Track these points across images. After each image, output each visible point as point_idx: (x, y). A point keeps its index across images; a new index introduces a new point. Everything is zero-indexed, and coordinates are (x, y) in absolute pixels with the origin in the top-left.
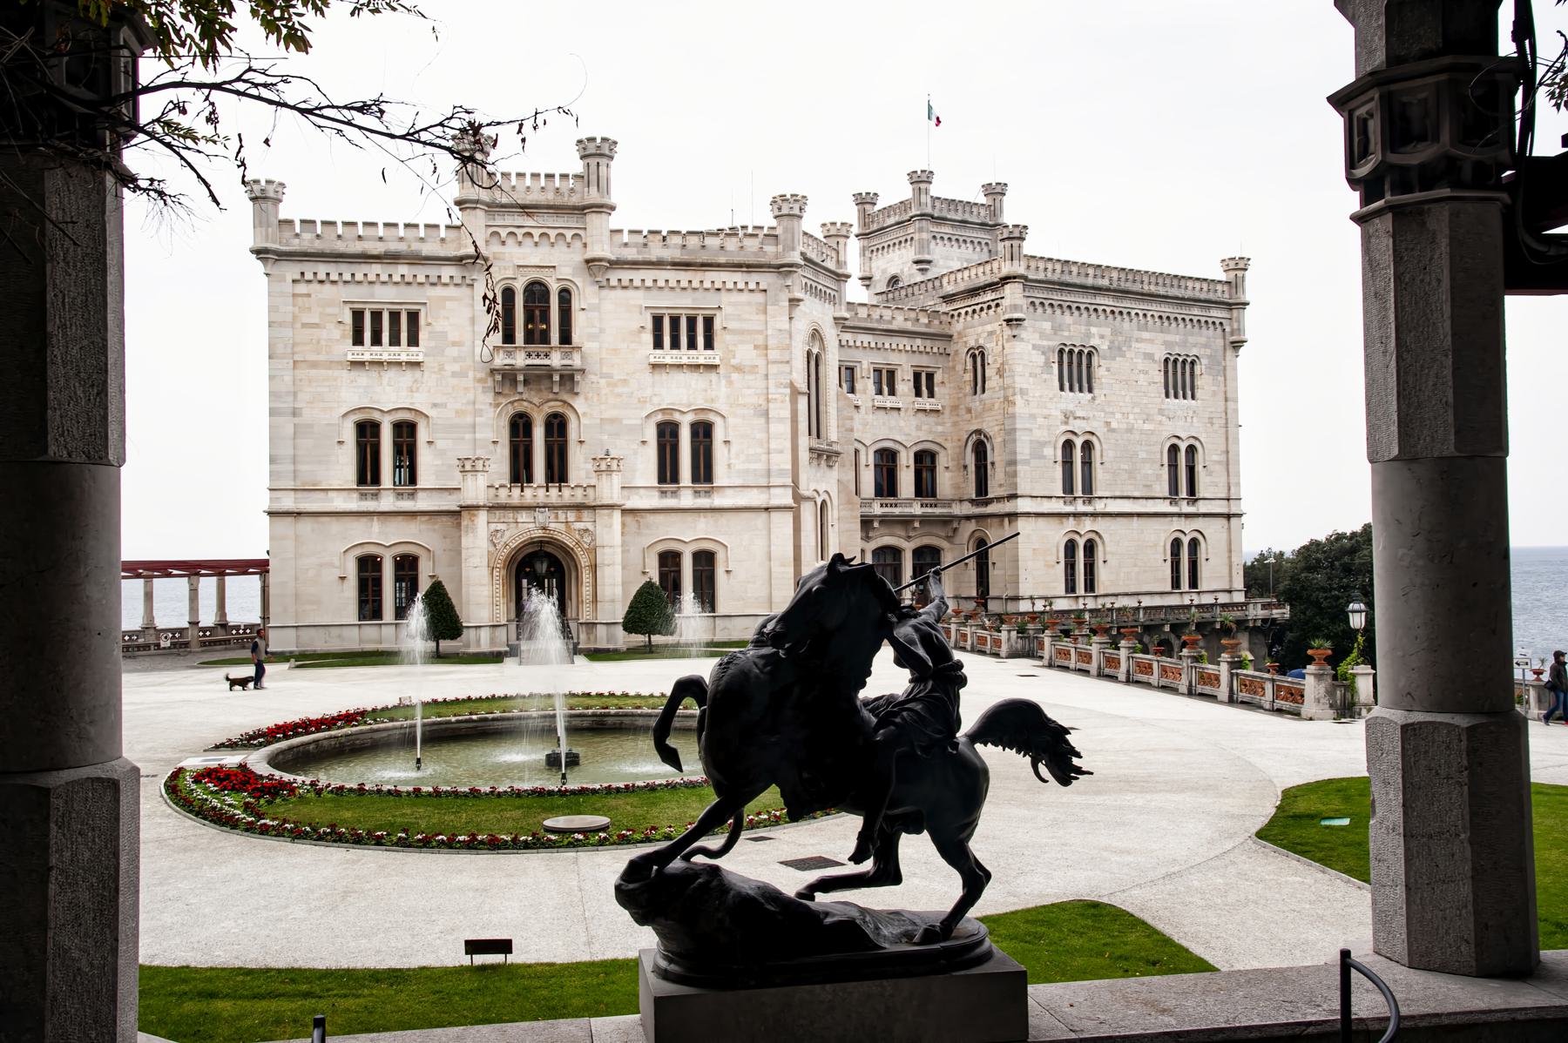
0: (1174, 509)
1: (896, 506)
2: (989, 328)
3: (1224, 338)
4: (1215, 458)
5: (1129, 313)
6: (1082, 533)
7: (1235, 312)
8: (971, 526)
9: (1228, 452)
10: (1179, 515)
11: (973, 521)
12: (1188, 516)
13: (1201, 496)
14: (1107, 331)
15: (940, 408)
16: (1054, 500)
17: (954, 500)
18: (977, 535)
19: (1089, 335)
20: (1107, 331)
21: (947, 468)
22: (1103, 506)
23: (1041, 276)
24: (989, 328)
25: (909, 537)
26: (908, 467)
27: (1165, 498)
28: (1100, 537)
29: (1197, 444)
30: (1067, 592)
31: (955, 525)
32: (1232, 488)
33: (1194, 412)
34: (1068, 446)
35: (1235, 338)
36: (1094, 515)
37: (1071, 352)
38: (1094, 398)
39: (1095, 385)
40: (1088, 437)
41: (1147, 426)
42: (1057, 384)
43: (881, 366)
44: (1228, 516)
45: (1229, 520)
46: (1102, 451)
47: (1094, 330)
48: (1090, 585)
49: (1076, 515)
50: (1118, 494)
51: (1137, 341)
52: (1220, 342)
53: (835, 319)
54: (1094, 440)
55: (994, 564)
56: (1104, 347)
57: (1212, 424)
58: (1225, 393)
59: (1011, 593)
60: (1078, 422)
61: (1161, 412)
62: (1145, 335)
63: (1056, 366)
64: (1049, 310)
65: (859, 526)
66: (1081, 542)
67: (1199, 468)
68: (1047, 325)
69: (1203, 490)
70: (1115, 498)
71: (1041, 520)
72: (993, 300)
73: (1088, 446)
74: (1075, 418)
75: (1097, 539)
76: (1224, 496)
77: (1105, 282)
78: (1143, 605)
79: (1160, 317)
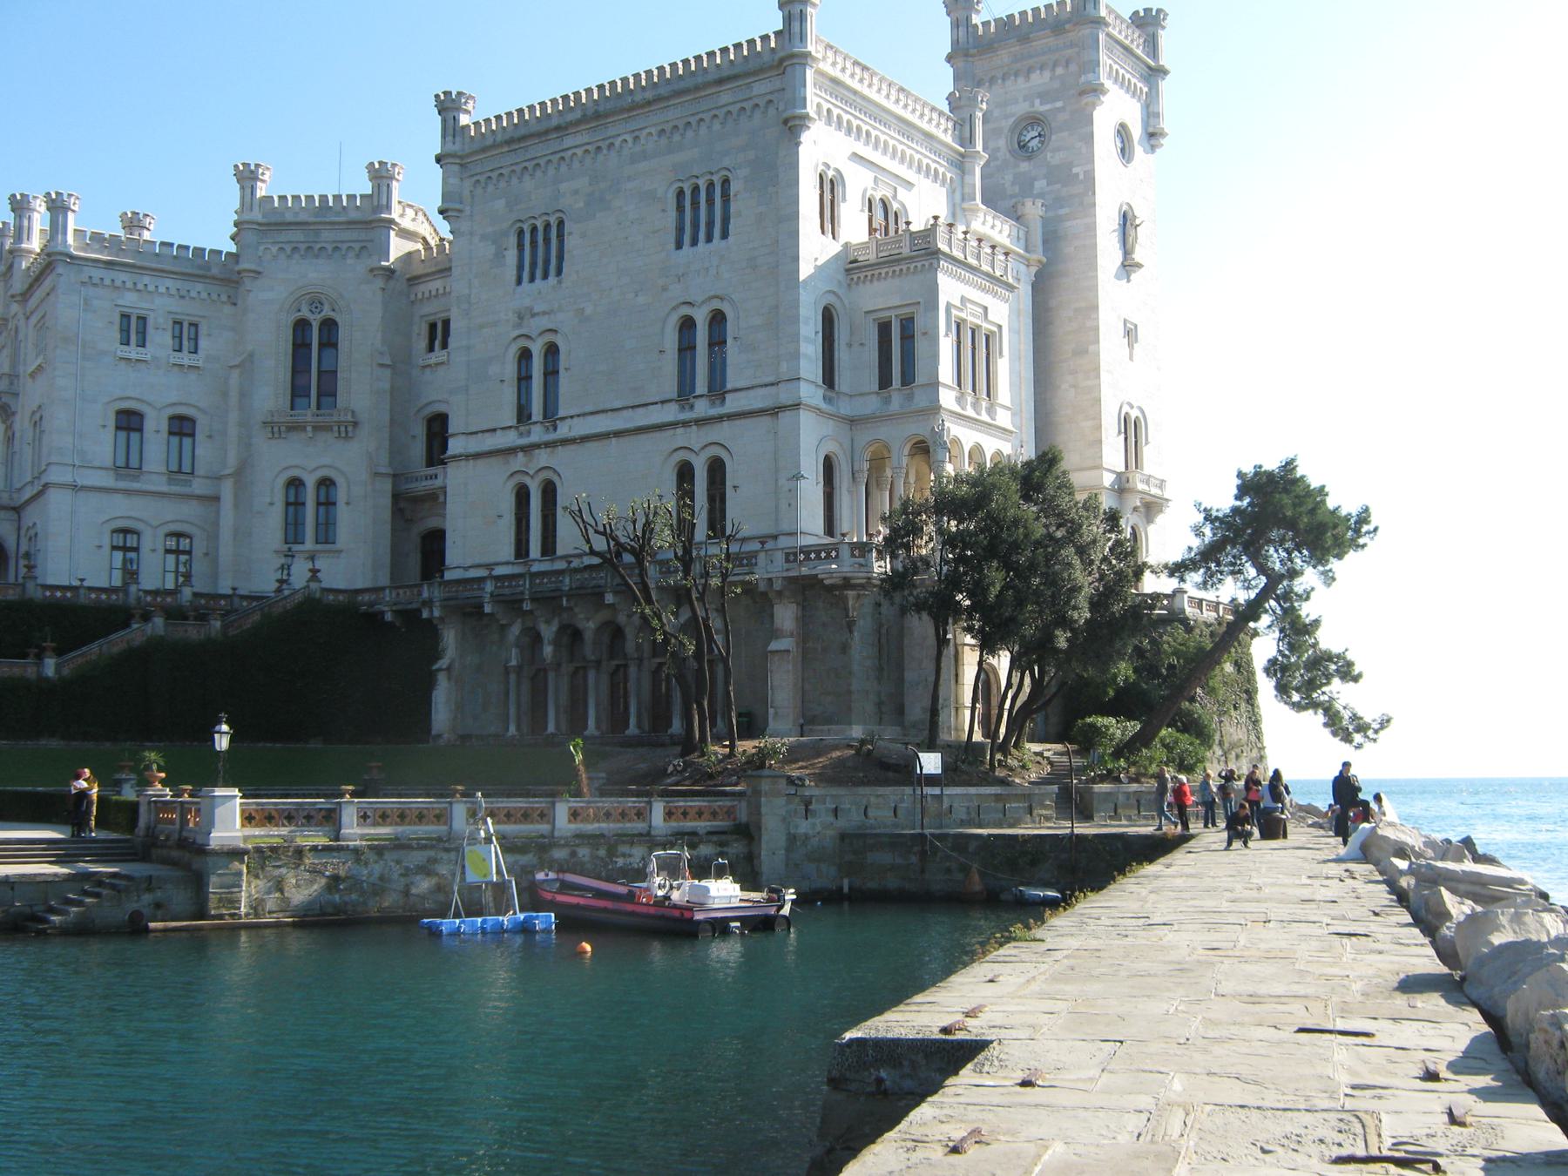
0: (687, 415)
6: (531, 473)
9: (777, 307)
10: (685, 424)
12: (701, 422)
16: (499, 433)
23: (489, 142)
27: (663, 402)
32: (784, 367)
37: (534, 229)
38: (560, 282)
41: (641, 299)
42: (511, 273)
44: (774, 411)
47: (563, 187)
48: (549, 547)
51: (629, 178)
53: (372, 270)
62: (643, 166)
63: (511, 256)
65: (387, 501)
68: (500, 204)
70: (584, 415)
71: (481, 463)
73: (552, 351)
74: (533, 315)
75: (555, 479)
78: (572, 565)
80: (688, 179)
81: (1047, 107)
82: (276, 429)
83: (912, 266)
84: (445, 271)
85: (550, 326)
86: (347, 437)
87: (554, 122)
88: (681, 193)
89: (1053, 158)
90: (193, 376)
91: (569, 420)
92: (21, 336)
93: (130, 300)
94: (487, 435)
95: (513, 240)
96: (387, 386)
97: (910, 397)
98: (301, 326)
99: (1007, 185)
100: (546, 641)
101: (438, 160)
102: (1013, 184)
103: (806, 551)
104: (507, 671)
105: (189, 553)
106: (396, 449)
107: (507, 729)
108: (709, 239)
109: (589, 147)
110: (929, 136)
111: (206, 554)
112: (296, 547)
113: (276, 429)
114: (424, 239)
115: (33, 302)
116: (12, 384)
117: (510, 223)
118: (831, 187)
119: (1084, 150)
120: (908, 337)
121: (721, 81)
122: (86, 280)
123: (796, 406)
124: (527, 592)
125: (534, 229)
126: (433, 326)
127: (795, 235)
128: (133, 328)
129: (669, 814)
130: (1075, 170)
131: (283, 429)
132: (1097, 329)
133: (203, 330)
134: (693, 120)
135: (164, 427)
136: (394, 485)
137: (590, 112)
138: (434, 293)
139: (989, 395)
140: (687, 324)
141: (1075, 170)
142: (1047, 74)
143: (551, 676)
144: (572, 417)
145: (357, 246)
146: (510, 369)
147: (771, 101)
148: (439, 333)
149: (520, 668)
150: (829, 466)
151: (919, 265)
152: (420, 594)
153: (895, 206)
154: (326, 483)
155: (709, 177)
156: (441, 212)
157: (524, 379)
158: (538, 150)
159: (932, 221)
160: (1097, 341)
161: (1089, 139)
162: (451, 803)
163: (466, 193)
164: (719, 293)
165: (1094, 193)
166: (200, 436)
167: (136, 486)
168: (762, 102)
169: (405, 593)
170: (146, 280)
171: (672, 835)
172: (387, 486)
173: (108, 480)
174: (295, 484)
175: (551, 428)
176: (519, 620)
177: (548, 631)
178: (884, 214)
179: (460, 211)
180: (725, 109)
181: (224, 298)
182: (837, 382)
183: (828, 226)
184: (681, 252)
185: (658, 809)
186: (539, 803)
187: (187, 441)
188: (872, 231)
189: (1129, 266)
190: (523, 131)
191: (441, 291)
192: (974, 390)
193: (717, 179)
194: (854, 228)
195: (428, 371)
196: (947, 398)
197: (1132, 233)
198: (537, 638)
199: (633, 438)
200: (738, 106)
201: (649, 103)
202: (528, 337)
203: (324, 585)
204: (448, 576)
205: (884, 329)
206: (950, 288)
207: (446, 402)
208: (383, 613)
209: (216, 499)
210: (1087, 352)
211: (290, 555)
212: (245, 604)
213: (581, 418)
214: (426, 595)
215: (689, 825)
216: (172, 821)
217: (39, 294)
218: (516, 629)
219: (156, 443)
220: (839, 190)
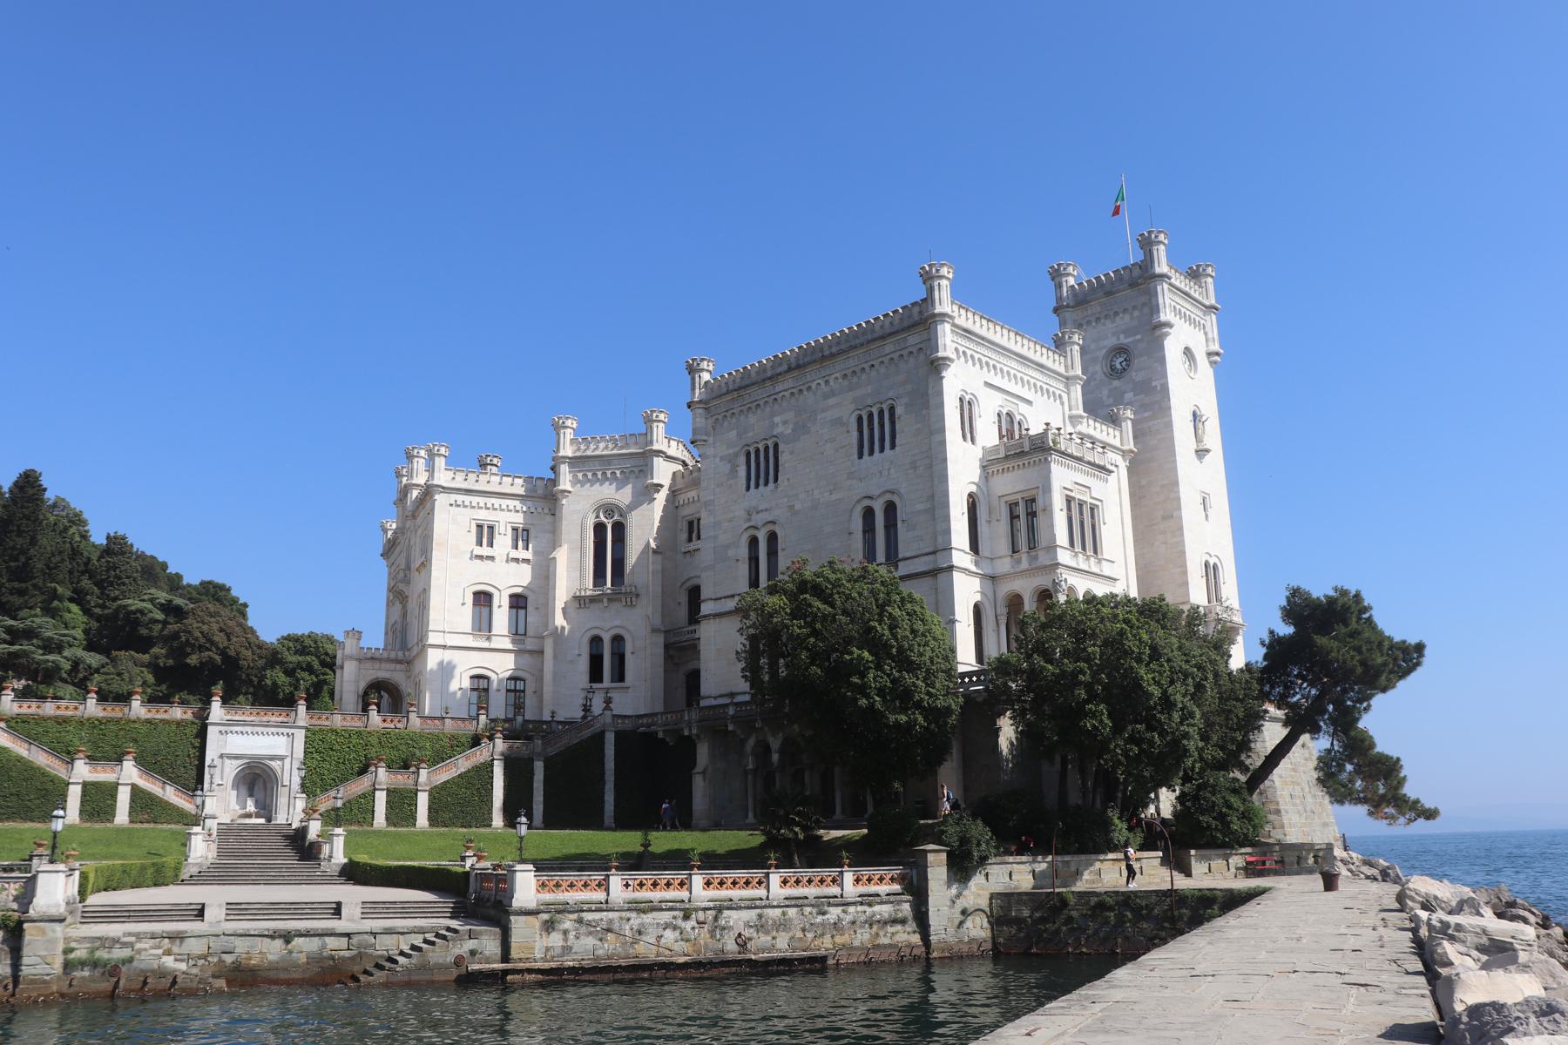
4: (920, 507)
5: (809, 388)
9: (932, 497)
14: (790, 415)
19: (773, 425)
20: (790, 415)
29: (895, 499)
32: (940, 539)
33: (892, 462)
34: (754, 542)
37: (757, 451)
38: (776, 487)
40: (770, 527)
41: (834, 497)
42: (743, 482)
47: (777, 419)
51: (823, 411)
54: (777, 529)
57: (915, 468)
60: (760, 514)
61: (850, 476)
62: (832, 401)
65: (661, 651)
68: (733, 433)
69: (903, 552)
73: (772, 538)
74: (758, 513)
76: (931, 549)
77: (785, 367)
80: (864, 408)
81: (1130, 340)
82: (582, 602)
83: (1032, 461)
84: (695, 483)
85: (770, 519)
86: (632, 605)
87: (769, 374)
88: (860, 419)
89: (1136, 375)
90: (525, 566)
92: (412, 543)
93: (484, 516)
95: (743, 459)
96: (659, 567)
97: (1036, 558)
98: (599, 529)
99: (1105, 398)
100: (773, 750)
101: (689, 407)
102: (1109, 397)
103: (963, 675)
104: (746, 773)
105: (524, 691)
106: (665, 612)
107: (747, 817)
108: (882, 450)
109: (794, 390)
110: (1041, 366)
111: (535, 692)
112: (595, 686)
113: (582, 602)
114: (684, 462)
115: (419, 520)
116: (405, 576)
117: (737, 449)
118: (967, 407)
119: (1159, 369)
120: (1032, 515)
121: (883, 338)
122: (453, 502)
123: (951, 568)
125: (757, 451)
126: (691, 524)
127: (943, 443)
128: (485, 533)
129: (857, 881)
130: (1154, 384)
131: (587, 601)
132: (1178, 499)
133: (532, 534)
134: (866, 366)
135: (506, 602)
136: (665, 639)
137: (793, 366)
138: (691, 500)
139: (1095, 552)
140: (869, 514)
141: (1154, 384)
142: (1127, 317)
143: (778, 776)
145: (636, 470)
146: (744, 551)
147: (921, 349)
148: (693, 528)
149: (755, 771)
150: (978, 611)
151: (1037, 459)
152: (682, 717)
153: (1018, 418)
154: (618, 640)
155: (879, 406)
156: (692, 443)
157: (754, 560)
158: (758, 393)
159: (1045, 427)
160: (1179, 508)
161: (1162, 361)
162: (690, 875)
163: (710, 428)
164: (890, 487)
165: (1169, 400)
166: (530, 608)
167: (486, 645)
168: (914, 350)
170: (493, 500)
171: (860, 896)
172: (660, 639)
173: (470, 641)
174: (596, 641)
176: (754, 736)
177: (775, 743)
178: (1008, 424)
179: (705, 441)
180: (888, 357)
181: (546, 511)
182: (980, 550)
183: (969, 436)
184: (862, 461)
185: (849, 877)
186: (758, 874)
187: (522, 612)
188: (1001, 437)
189: (1201, 453)
190: (747, 382)
191: (696, 498)
192: (1084, 548)
193: (885, 406)
194: (988, 434)
195: (688, 555)
196: (1064, 557)
197: (1200, 425)
198: (767, 749)
200: (898, 354)
201: (833, 355)
202: (755, 527)
203: (614, 713)
204: (703, 703)
205: (1012, 506)
206: (1062, 477)
207: (699, 577)
208: (656, 733)
209: (542, 652)
210: (1172, 516)
211: (591, 691)
212: (560, 727)
214: (686, 718)
215: (873, 889)
216: (491, 889)
217: (422, 514)
218: (751, 742)
219: (501, 616)
220: (976, 409)
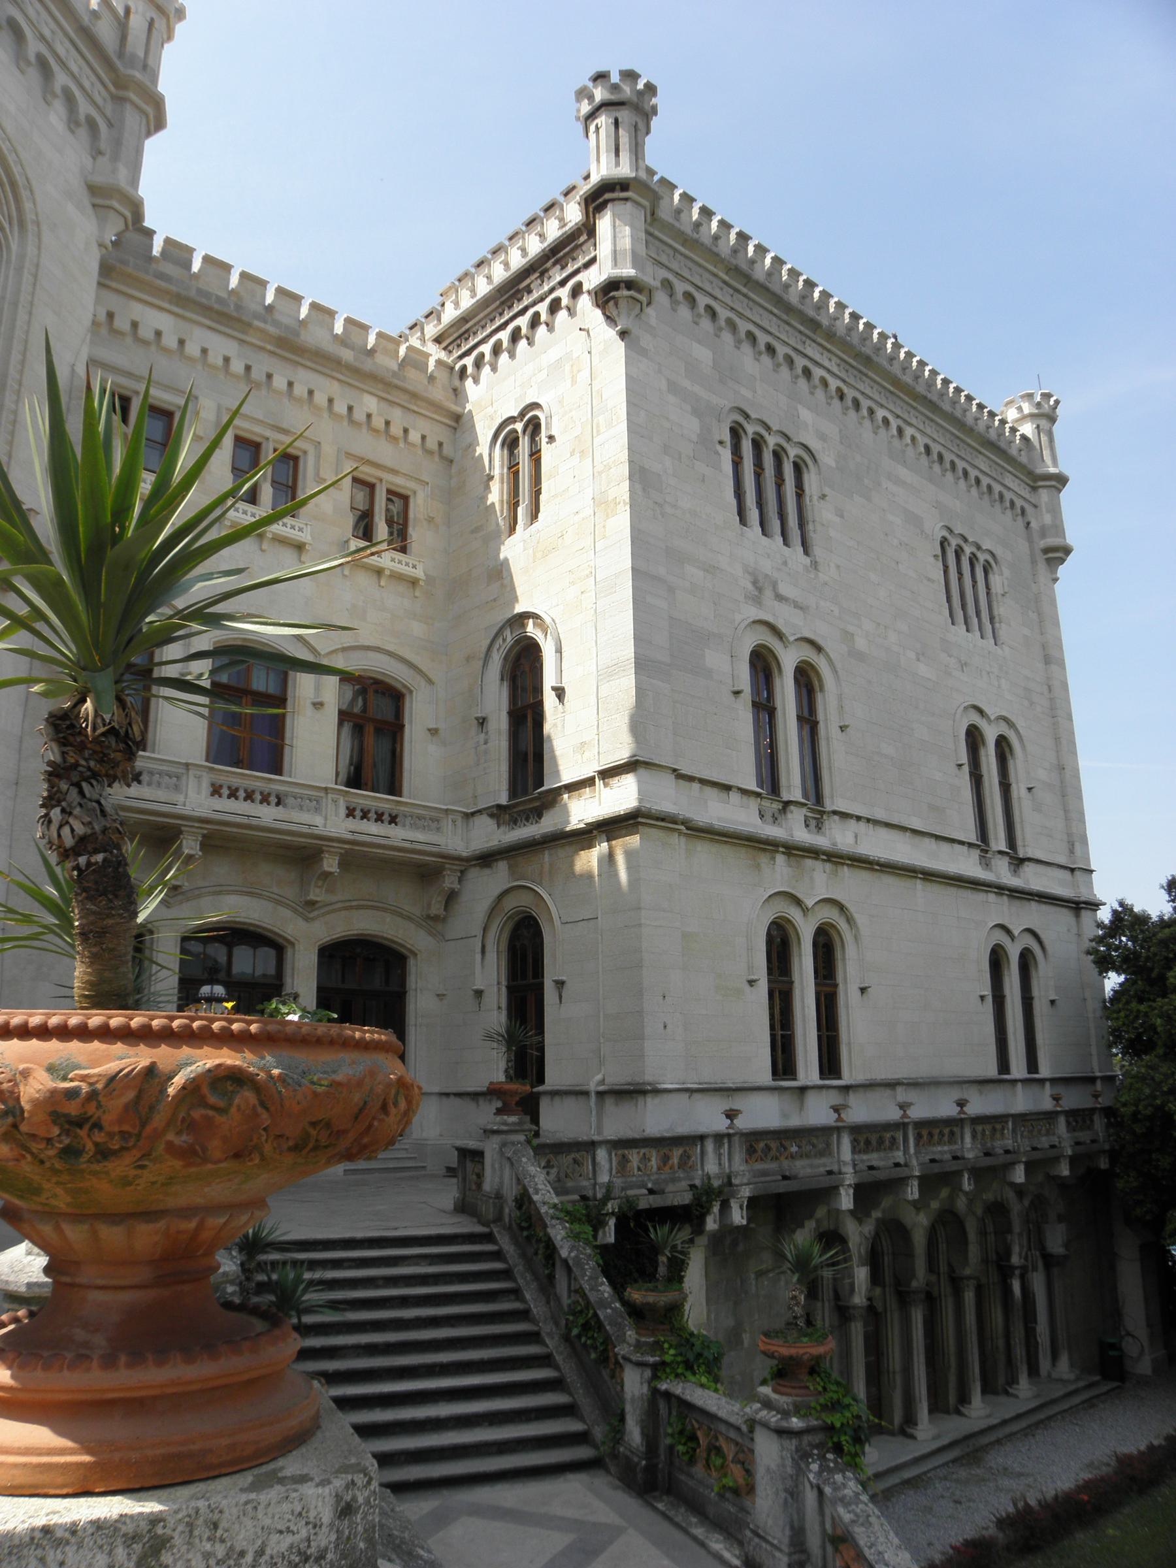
1: (265, 799)
2: (553, 354)
3: (1030, 540)
5: (871, 412)
6: (809, 903)
7: (1044, 496)
8: (497, 879)
9: (1061, 768)
10: (1000, 889)
11: (502, 866)
13: (1030, 855)
15: (419, 573)
16: (735, 797)
17: (447, 812)
18: (510, 903)
21: (434, 732)
22: (850, 839)
24: (553, 354)
25: (311, 904)
26: (318, 705)
27: (970, 845)
28: (850, 920)
30: (775, 1073)
31: (449, 881)
35: (1051, 541)
36: (835, 858)
38: (815, 565)
39: (815, 538)
40: (808, 654)
41: (923, 669)
43: (268, 433)
45: (1078, 916)
46: (840, 697)
47: (805, 415)
49: (793, 851)
50: (880, 815)
52: (1023, 547)
55: (560, 984)
56: (827, 459)
58: (1044, 647)
59: (616, 1075)
62: (903, 472)
64: (706, 324)
66: (806, 931)
67: (1018, 791)
72: (562, 283)
73: (806, 679)
75: (842, 925)
76: (1062, 860)
79: (927, 449)
91: (853, 822)
94: (710, 792)
95: (727, 437)
124: (914, 1162)
144: (859, 818)
169: (645, 1159)
175: (813, 823)
199: (952, 891)
213: (871, 826)
